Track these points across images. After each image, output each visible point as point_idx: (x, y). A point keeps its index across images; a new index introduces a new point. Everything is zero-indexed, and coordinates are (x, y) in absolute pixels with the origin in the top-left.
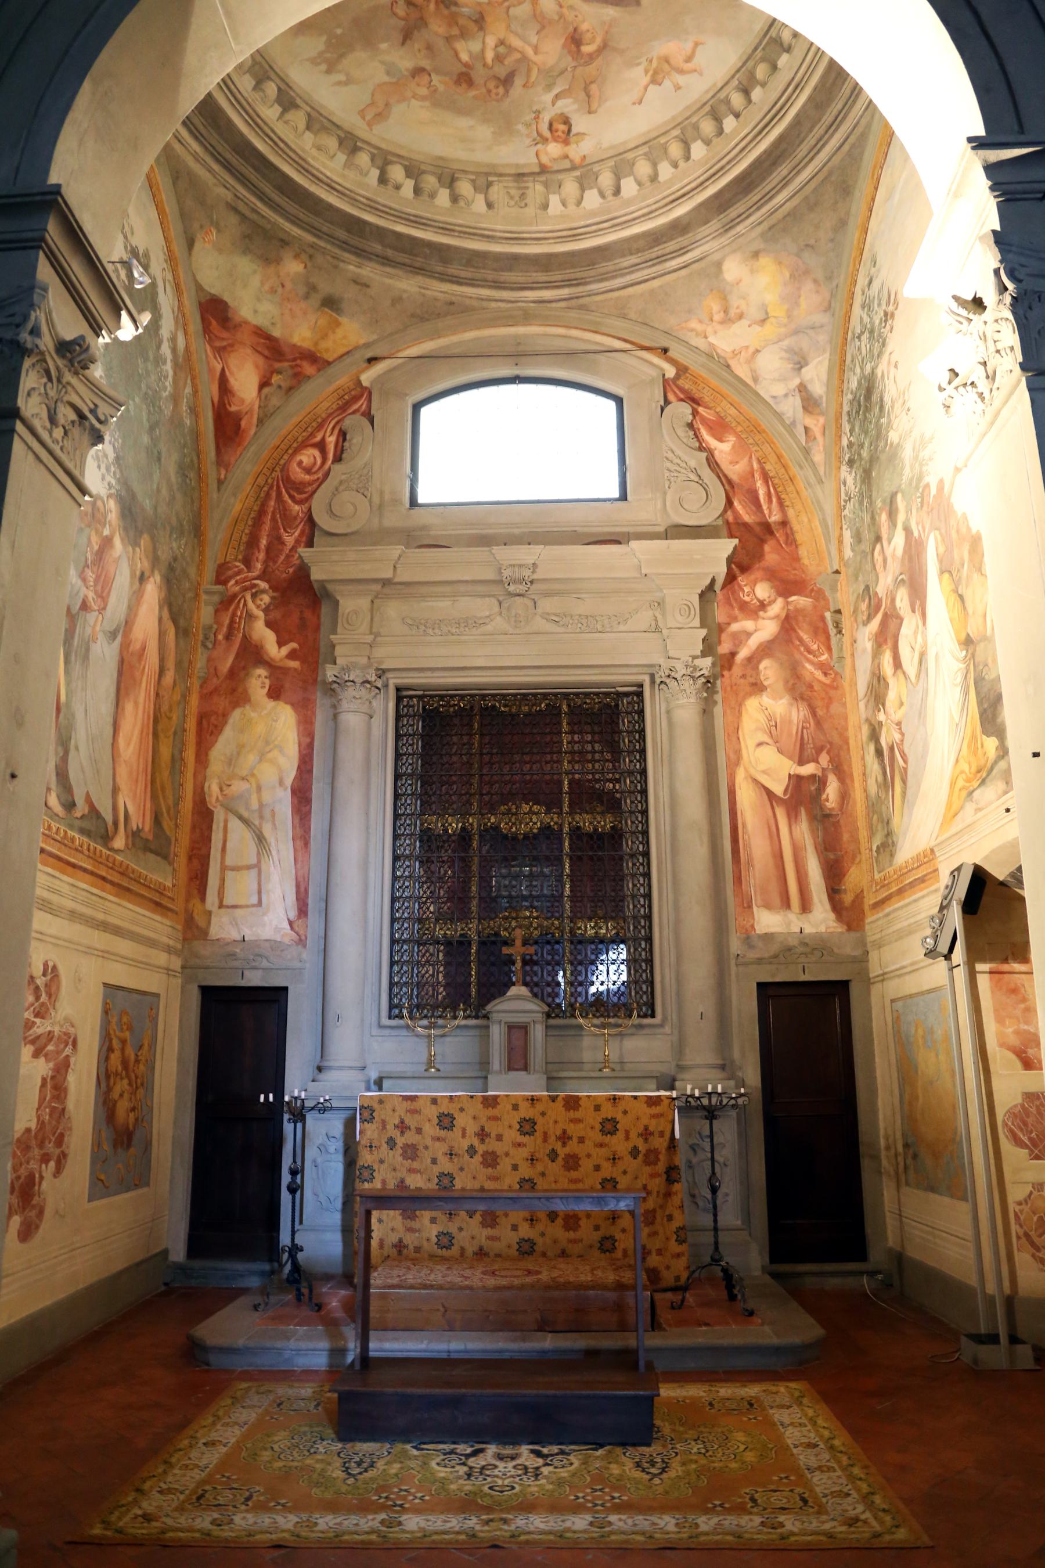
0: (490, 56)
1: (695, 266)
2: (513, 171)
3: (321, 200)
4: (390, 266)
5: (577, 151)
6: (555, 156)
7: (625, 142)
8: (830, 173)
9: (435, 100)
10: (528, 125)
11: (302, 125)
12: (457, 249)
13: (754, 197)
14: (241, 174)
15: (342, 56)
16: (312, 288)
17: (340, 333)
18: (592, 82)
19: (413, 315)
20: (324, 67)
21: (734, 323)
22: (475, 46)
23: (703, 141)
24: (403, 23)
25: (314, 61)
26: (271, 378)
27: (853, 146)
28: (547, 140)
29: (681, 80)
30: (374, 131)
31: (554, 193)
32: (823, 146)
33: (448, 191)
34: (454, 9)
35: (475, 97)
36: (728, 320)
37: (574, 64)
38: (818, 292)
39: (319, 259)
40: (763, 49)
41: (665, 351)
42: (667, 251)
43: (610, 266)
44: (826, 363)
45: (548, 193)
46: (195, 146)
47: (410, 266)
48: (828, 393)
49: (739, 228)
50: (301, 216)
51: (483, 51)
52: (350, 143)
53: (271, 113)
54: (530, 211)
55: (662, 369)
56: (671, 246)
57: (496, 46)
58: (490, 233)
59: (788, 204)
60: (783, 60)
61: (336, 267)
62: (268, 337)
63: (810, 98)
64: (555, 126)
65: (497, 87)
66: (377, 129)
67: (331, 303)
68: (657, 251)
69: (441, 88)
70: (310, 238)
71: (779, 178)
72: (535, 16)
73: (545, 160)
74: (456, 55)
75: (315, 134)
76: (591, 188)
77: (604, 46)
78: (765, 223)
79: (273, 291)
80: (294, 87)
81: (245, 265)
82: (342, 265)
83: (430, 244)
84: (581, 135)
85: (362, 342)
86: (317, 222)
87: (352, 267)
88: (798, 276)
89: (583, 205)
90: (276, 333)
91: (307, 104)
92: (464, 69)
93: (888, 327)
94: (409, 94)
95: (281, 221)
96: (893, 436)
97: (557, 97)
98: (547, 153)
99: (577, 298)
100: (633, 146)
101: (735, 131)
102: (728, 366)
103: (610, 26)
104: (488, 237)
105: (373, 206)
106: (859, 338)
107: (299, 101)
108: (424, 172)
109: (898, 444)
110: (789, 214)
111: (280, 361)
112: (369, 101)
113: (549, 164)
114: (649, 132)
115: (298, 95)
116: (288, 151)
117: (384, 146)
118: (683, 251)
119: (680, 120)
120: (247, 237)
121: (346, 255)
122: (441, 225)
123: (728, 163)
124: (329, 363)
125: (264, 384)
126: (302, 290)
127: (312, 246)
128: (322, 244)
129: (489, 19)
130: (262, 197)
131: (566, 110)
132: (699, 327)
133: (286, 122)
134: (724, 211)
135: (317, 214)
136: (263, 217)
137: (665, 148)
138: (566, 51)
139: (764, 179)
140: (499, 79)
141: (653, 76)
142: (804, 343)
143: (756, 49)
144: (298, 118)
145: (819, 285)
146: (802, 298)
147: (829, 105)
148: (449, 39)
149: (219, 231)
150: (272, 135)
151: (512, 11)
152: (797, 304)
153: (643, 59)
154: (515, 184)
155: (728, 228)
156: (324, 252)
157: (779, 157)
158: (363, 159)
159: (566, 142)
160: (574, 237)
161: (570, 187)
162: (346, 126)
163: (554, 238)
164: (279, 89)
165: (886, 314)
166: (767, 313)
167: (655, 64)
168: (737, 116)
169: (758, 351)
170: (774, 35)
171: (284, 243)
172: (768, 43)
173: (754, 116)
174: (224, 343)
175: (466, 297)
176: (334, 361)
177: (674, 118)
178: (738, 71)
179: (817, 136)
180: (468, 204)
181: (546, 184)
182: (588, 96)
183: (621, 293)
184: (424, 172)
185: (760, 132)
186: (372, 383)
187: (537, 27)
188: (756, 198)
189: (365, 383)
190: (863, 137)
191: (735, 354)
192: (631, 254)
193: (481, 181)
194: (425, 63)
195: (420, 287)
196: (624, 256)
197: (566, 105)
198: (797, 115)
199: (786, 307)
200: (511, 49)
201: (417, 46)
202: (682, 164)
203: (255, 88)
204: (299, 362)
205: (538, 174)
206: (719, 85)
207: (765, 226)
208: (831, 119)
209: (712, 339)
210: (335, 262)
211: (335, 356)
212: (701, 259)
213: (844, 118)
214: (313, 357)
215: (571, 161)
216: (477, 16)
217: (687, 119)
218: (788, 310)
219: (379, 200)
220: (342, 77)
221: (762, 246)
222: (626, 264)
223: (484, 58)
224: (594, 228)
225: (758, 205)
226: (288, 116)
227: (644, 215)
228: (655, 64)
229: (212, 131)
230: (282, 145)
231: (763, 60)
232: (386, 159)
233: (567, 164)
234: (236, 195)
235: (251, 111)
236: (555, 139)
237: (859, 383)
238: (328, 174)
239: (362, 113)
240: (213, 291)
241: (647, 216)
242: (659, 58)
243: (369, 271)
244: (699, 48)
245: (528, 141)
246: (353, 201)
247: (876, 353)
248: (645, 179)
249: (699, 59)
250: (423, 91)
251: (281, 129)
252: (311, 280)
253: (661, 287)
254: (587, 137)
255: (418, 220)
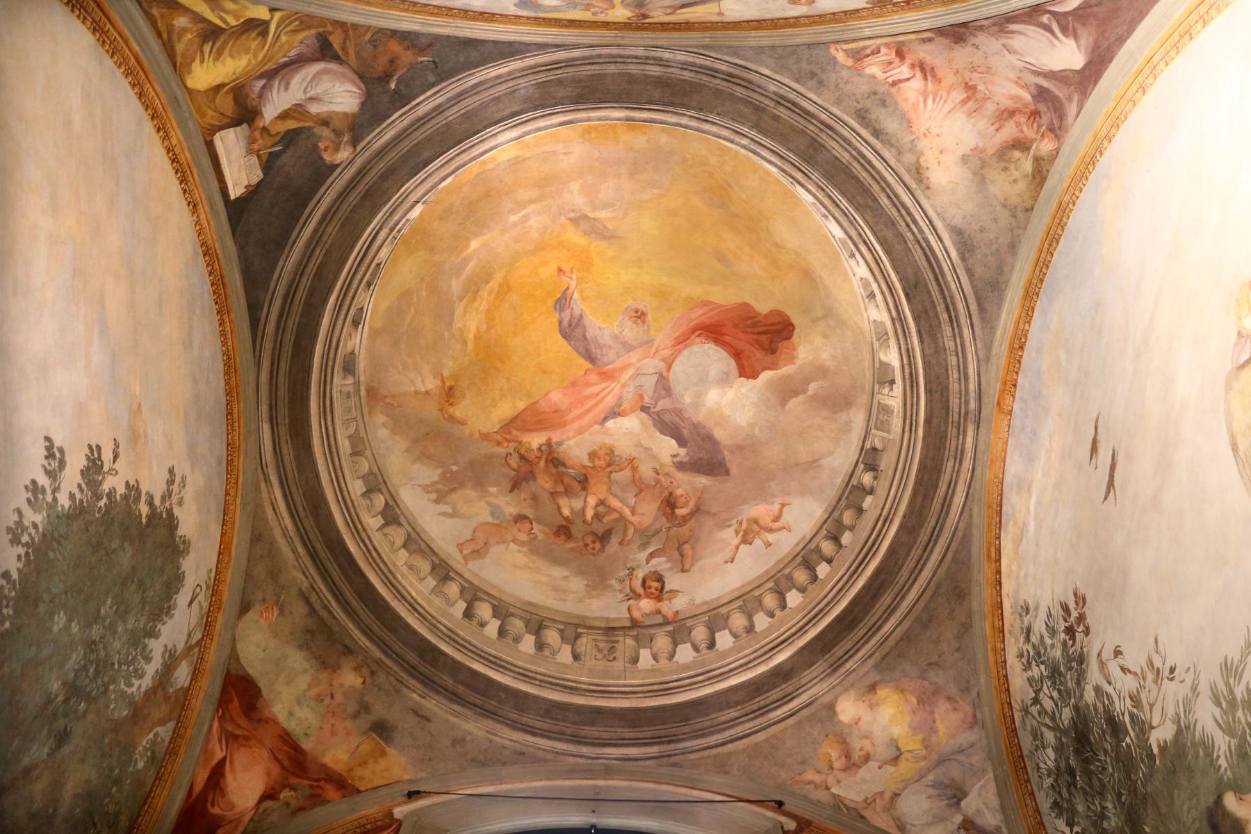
0: (590, 514)
1: (805, 712)
2: (603, 625)
3: (400, 618)
4: (458, 703)
5: (670, 607)
6: (647, 611)
7: (719, 598)
8: (938, 586)
9: (534, 548)
10: (621, 581)
11: (400, 541)
12: (536, 697)
13: (860, 631)
14: (326, 570)
15: (453, 490)
16: (365, 708)
17: (383, 763)
18: (685, 543)
19: (473, 760)
20: (434, 496)
21: (860, 767)
22: (577, 504)
23: (797, 589)
24: (514, 473)
25: (426, 489)
26: (281, 792)
27: (956, 552)
28: (640, 596)
29: (770, 537)
30: (469, 566)
31: (645, 647)
32: (925, 564)
33: (533, 637)
34: (561, 469)
35: (572, 549)
36: (852, 765)
37: (669, 525)
38: (955, 709)
39: (381, 678)
40: (847, 498)
41: (780, 804)
42: (770, 700)
43: (704, 722)
44: (992, 784)
45: (639, 647)
46: (288, 521)
47: (481, 708)
48: (1006, 820)
49: (848, 665)
50: (375, 628)
51: (584, 509)
52: (443, 572)
53: (373, 522)
54: (618, 665)
55: (781, 823)
56: (775, 694)
57: (597, 506)
58: (574, 685)
59: (899, 629)
60: (868, 502)
61: (398, 691)
62: (296, 748)
63: (901, 526)
64: (649, 583)
65: (594, 542)
66: (472, 565)
67: (381, 729)
68: (759, 701)
69: (541, 536)
70: (377, 653)
71: (884, 608)
72: (634, 481)
73: (636, 615)
74: (559, 508)
75: (410, 554)
76: (685, 642)
77: (697, 510)
78: (877, 654)
79: (319, 699)
80: (402, 506)
81: (297, 660)
82: (404, 690)
83: (506, 689)
84: (674, 592)
85: (407, 777)
86: (391, 640)
87: (415, 695)
88: (926, 700)
89: (675, 659)
90: (307, 745)
91: (409, 524)
92: (564, 523)
93: (1079, 636)
94: (509, 537)
95: (351, 626)
96: (1161, 734)
97: (651, 555)
98: (639, 609)
99: (669, 756)
100: (726, 600)
101: (830, 576)
102: (862, 817)
103: (702, 493)
104: (571, 688)
105: (452, 638)
106: (1036, 701)
107: (402, 519)
108: (512, 615)
109: (1179, 732)
110: (901, 639)
111: (298, 776)
112: (469, 537)
113: (641, 619)
114: (742, 586)
115: (403, 513)
116: (379, 561)
117: (476, 583)
118: (787, 698)
119: (773, 573)
120: (309, 632)
121: (413, 681)
122: (521, 671)
123: (827, 605)
124: (358, 791)
125: (268, 796)
126: (352, 707)
127: (378, 662)
128: (389, 663)
129: (592, 481)
130: (339, 596)
131: (659, 569)
132: (817, 778)
133: (385, 535)
134: (829, 651)
135: (392, 630)
136: (334, 617)
137: (759, 600)
138: (661, 513)
139: (868, 612)
140: (596, 535)
141: (744, 536)
142: (955, 772)
143: (840, 500)
144: (399, 535)
145: (956, 701)
146: (938, 722)
147: (921, 527)
148: (553, 494)
149: (281, 613)
150: (368, 542)
151: (613, 476)
152: (933, 730)
153: (734, 522)
154: (605, 638)
155: (835, 668)
156: (388, 671)
157: (880, 588)
158: (453, 589)
159: (659, 599)
160: (666, 691)
161: (662, 642)
162: (442, 555)
163: (643, 692)
164: (387, 504)
165: (1070, 631)
166: (898, 748)
167: (745, 525)
168: (829, 561)
169: (896, 795)
170: (855, 483)
171: (348, 651)
172: (850, 492)
173: (846, 560)
174: (239, 732)
175: (539, 749)
176: (367, 790)
177: (766, 572)
178: (825, 522)
179: (916, 557)
180: (554, 653)
181: (637, 639)
182: (682, 555)
183: (721, 749)
184: (512, 615)
185: (855, 571)
186: (405, 817)
187: (635, 490)
188: (862, 633)
189: (396, 816)
190: (967, 538)
191: (868, 803)
192: (730, 708)
193: (570, 632)
194: (528, 512)
195: (488, 732)
196: (721, 710)
197: (659, 564)
198: (891, 545)
199: (920, 737)
200: (610, 509)
201: (523, 495)
202: (778, 613)
203: (364, 495)
204: (322, 783)
205: (629, 628)
206: (808, 538)
207: (878, 655)
208: (926, 538)
209: (834, 790)
210: (399, 685)
211: (369, 786)
212: (810, 704)
213: (941, 530)
214: (343, 785)
215: (664, 616)
216: (582, 478)
217: (779, 572)
218: (924, 740)
219: (461, 633)
220: (449, 509)
221: (878, 678)
222: (723, 719)
223: (584, 516)
224: (687, 681)
225: (866, 638)
226: (388, 530)
227: (741, 666)
228: (745, 525)
229: (310, 518)
230: (374, 554)
231: (848, 507)
232: (475, 595)
233: (659, 619)
234: (312, 586)
235: (353, 514)
236: (648, 596)
237: (1059, 749)
238: (414, 594)
239: (460, 547)
240: (250, 671)
241: (745, 666)
242: (748, 520)
243: (433, 705)
244: (786, 509)
245: (620, 596)
246: (433, 628)
247: (1070, 684)
248: (741, 631)
249: (787, 517)
250: (523, 537)
251: (377, 539)
252: (366, 698)
253: (766, 740)
254: (680, 594)
255: (498, 662)
